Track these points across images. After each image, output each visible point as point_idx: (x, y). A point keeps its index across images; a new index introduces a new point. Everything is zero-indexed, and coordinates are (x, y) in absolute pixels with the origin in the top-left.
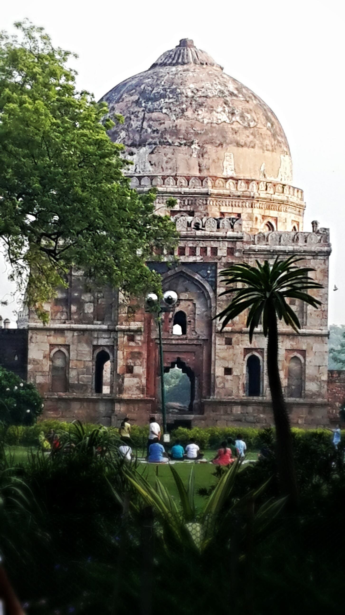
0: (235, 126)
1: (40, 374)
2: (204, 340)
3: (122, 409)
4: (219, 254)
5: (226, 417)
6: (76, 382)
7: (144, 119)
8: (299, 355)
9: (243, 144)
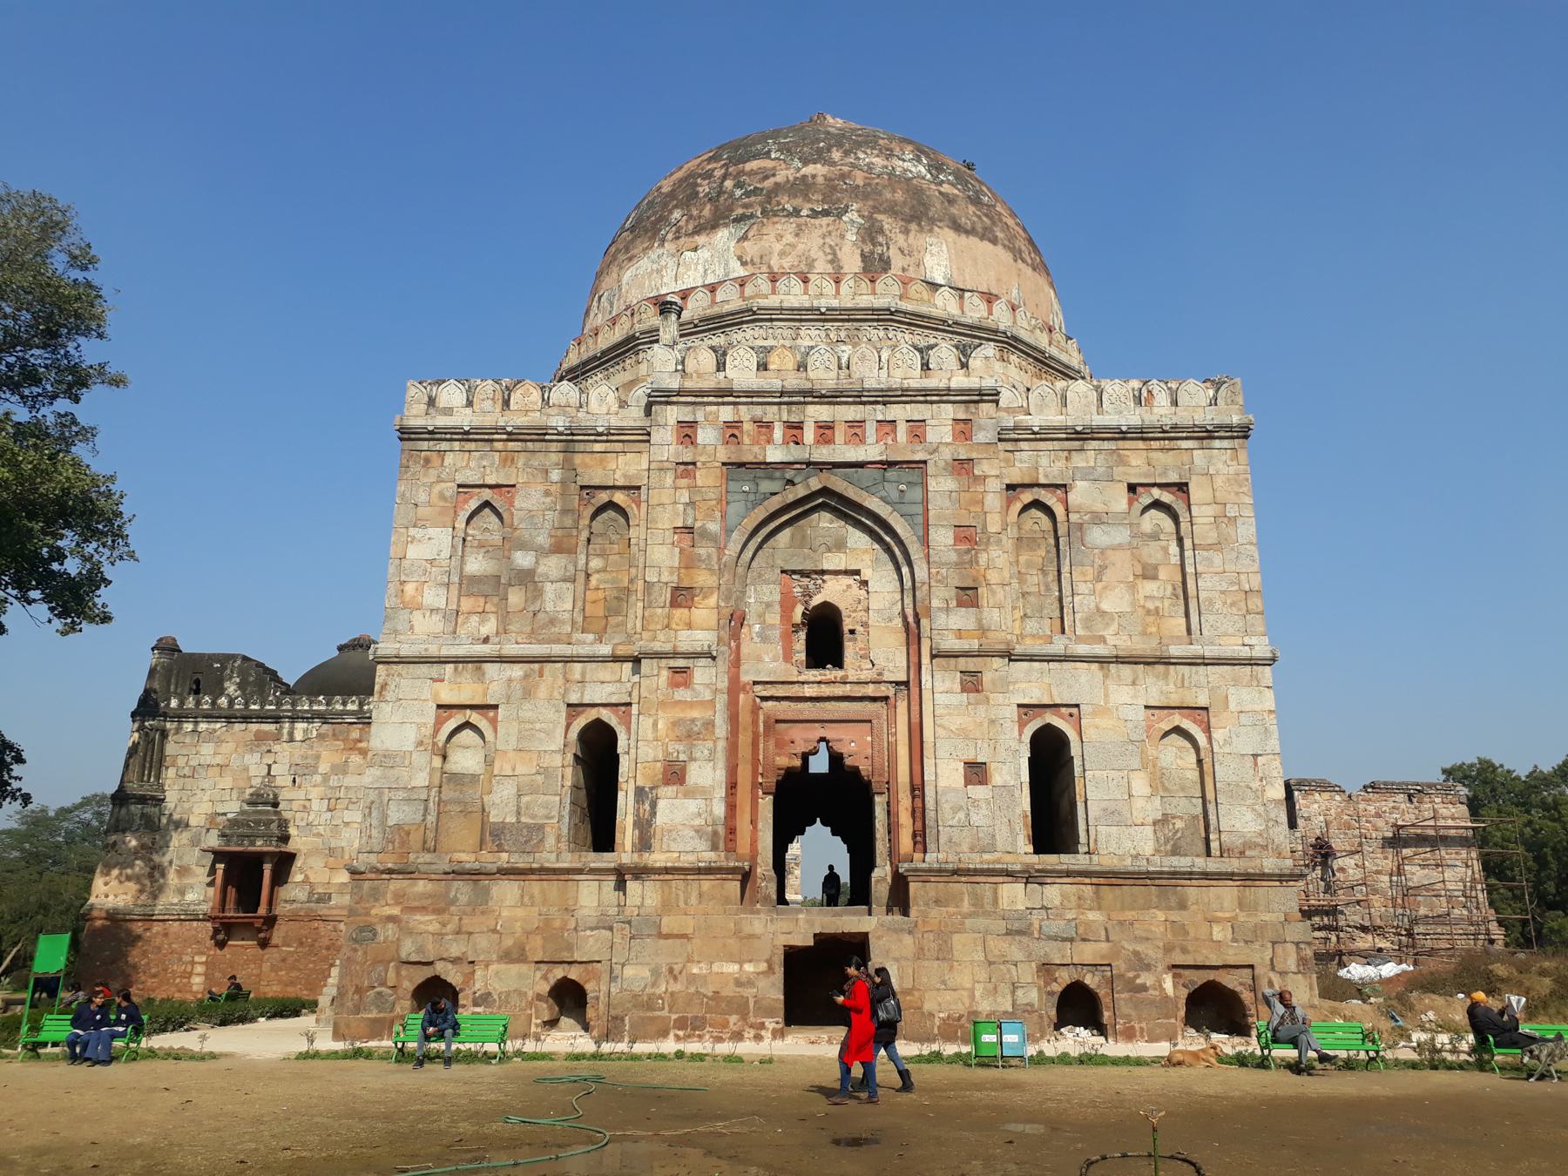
0: (946, 188)
1: (402, 794)
2: (897, 683)
3: (648, 902)
4: (932, 436)
5: (981, 922)
6: (511, 819)
7: (724, 178)
8: (1187, 725)
9: (969, 227)
